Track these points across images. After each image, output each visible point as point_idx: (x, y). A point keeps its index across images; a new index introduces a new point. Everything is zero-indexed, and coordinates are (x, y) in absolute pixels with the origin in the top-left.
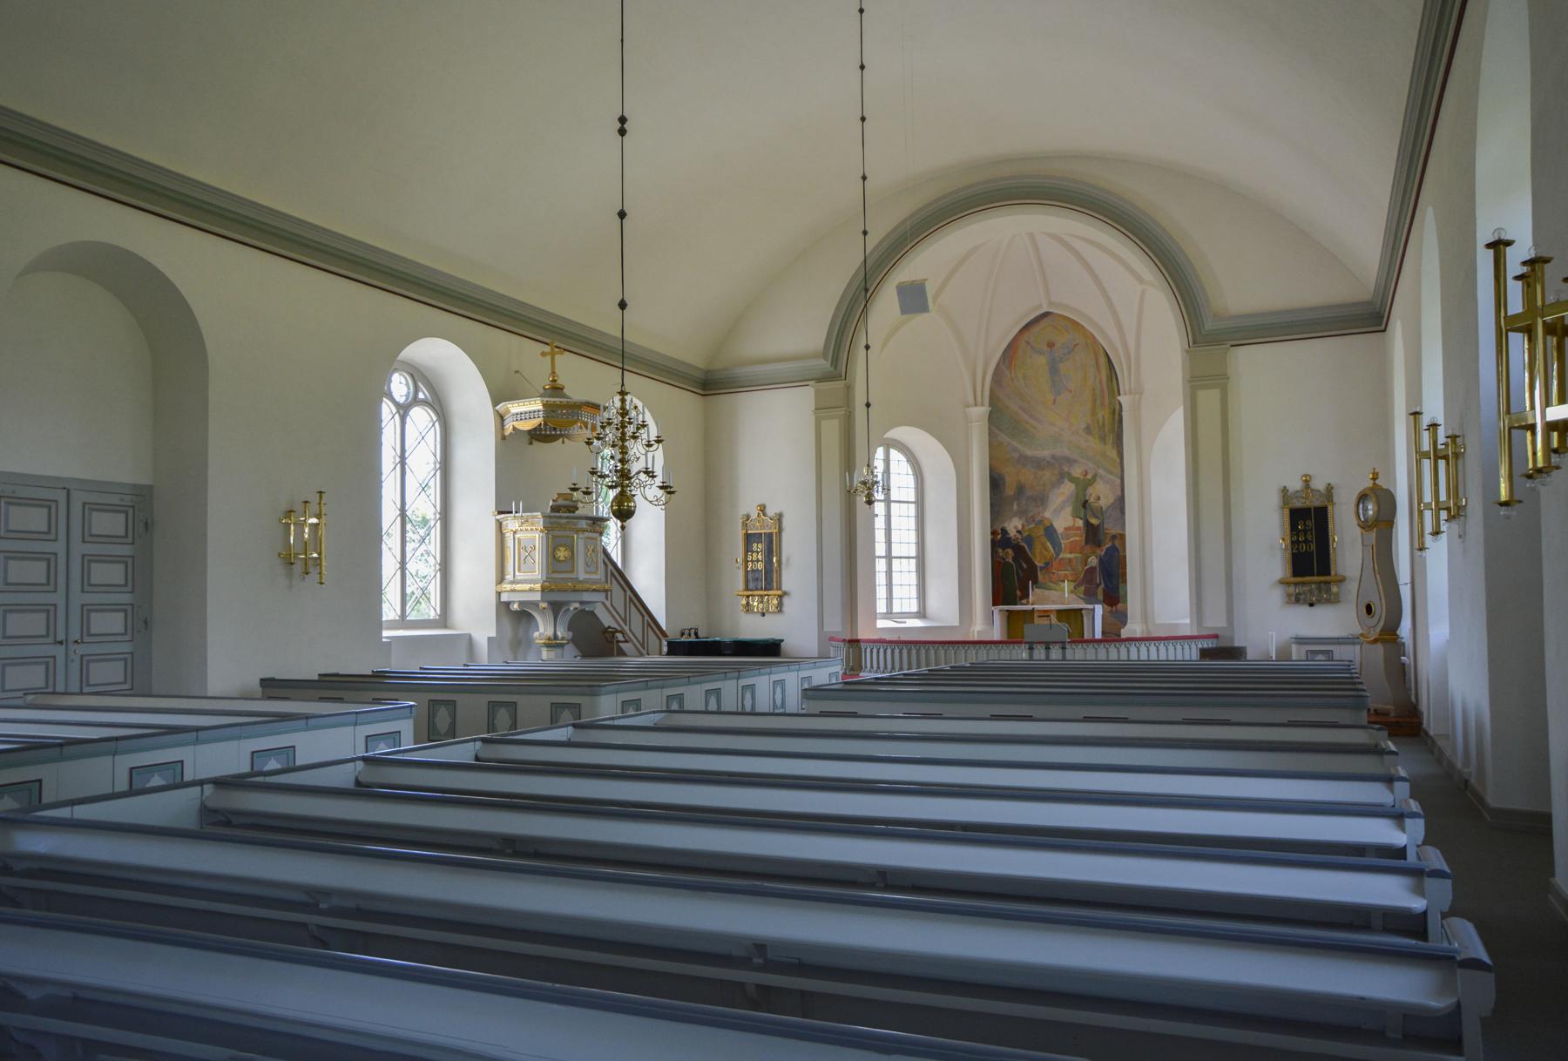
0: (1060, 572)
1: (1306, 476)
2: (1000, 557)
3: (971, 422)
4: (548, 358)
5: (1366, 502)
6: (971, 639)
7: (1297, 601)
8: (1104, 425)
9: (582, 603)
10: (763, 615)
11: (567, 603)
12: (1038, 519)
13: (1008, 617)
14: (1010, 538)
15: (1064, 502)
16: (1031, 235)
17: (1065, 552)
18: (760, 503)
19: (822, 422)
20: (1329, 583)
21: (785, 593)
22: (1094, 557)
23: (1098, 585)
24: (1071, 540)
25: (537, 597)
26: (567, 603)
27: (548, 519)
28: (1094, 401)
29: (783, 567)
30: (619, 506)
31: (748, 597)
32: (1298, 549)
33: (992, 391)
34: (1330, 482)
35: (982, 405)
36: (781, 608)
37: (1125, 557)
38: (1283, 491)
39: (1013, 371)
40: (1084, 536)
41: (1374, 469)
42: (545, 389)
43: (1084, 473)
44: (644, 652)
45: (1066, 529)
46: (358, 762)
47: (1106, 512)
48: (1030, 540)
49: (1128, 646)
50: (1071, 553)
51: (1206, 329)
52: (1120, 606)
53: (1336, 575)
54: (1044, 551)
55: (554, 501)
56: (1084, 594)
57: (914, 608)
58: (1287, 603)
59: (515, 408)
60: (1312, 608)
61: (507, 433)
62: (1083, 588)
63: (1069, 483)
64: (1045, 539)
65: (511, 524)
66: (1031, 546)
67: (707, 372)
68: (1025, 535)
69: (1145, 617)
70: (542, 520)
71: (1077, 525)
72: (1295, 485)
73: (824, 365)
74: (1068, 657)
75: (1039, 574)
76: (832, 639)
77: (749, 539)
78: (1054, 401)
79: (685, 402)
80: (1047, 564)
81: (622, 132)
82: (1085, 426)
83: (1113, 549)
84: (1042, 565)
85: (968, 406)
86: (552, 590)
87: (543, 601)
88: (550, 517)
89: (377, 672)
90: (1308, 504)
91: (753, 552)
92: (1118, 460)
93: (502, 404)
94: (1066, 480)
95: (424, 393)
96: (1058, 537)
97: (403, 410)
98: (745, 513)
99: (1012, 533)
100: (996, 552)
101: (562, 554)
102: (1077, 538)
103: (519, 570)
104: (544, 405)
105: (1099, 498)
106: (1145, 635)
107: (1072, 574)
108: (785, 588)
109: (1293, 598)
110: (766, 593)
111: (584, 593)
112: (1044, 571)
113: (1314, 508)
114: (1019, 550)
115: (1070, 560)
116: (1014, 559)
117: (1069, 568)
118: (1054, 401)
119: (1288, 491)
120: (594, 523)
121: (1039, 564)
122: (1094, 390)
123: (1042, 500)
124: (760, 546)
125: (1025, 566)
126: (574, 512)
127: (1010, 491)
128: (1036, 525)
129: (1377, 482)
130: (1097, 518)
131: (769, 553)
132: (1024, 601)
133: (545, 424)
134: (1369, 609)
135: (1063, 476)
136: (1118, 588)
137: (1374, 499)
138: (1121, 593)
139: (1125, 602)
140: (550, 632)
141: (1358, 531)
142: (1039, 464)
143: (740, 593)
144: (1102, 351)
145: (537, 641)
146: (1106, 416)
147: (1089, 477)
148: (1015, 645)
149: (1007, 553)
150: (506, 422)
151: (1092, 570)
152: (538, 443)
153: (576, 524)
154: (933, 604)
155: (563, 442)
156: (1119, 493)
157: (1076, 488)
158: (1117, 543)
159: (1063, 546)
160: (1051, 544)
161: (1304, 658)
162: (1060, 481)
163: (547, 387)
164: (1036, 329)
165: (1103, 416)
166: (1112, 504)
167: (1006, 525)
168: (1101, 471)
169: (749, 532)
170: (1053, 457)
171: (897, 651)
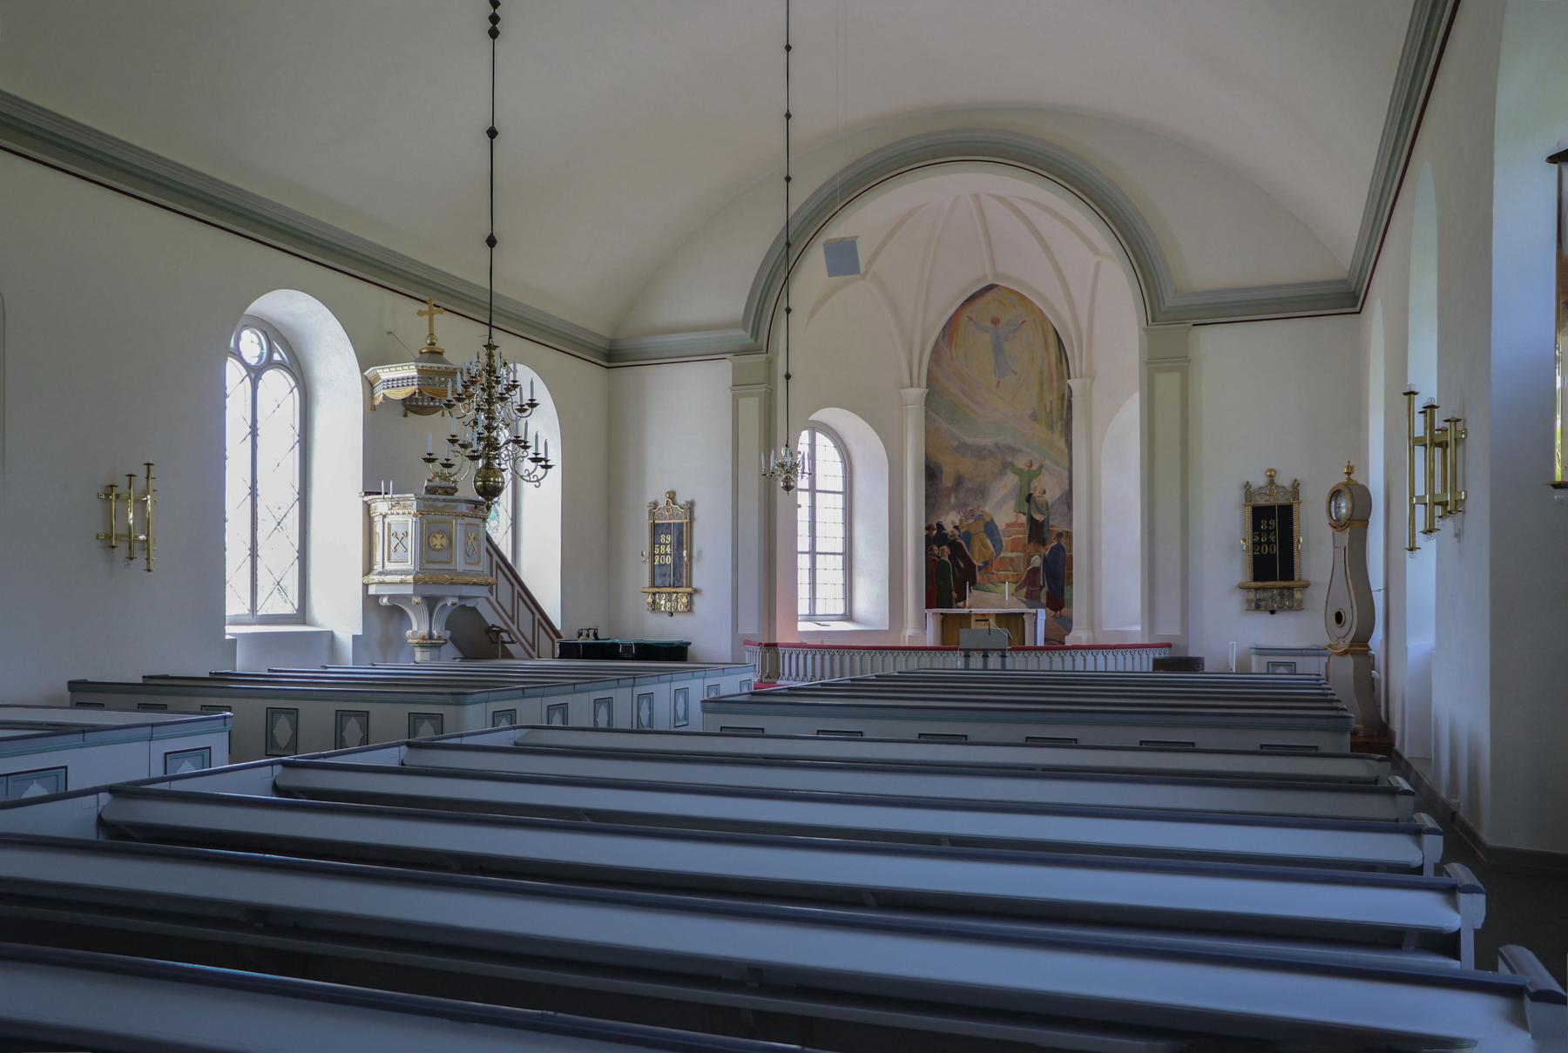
1: (1270, 470)
3: (906, 405)
4: (426, 317)
5: (1339, 498)
6: (902, 645)
7: (1258, 607)
8: (1051, 412)
9: (461, 598)
10: (671, 614)
11: (442, 598)
12: (977, 513)
13: (943, 621)
14: (946, 534)
16: (976, 197)
18: (669, 490)
19: (742, 401)
20: (1292, 588)
21: (696, 591)
23: (1042, 588)
24: (1014, 537)
25: (409, 590)
26: (442, 598)
27: (421, 501)
28: (1042, 384)
29: (694, 561)
30: (484, 482)
31: (654, 594)
32: (1260, 551)
33: (929, 369)
34: (1297, 478)
35: (919, 386)
36: (691, 607)
37: (1071, 557)
38: (1245, 487)
40: (1028, 533)
41: (1349, 462)
42: (421, 353)
43: (1029, 464)
44: (535, 654)
45: (1007, 525)
46: (101, 795)
47: (1052, 505)
48: (968, 536)
50: (1013, 551)
52: (1064, 610)
53: (1300, 580)
54: (983, 548)
55: (429, 481)
56: (1026, 597)
57: (840, 610)
58: (1247, 610)
59: (386, 373)
60: (1274, 616)
61: (377, 402)
62: (1024, 590)
64: (984, 536)
65: (381, 506)
66: (968, 543)
67: (612, 341)
68: (962, 531)
69: (1092, 624)
70: (415, 503)
72: (1259, 481)
73: (744, 336)
74: (1008, 666)
75: (977, 574)
76: (747, 643)
77: (656, 529)
78: (998, 383)
79: (587, 375)
80: (986, 563)
81: (494, 33)
83: (1059, 548)
84: (981, 565)
85: (903, 387)
86: (426, 583)
87: (415, 594)
88: (426, 500)
89: (216, 674)
90: (1272, 501)
91: (660, 544)
92: (1066, 450)
93: (372, 369)
95: (281, 356)
96: (998, 534)
97: (255, 374)
98: (653, 500)
99: (949, 529)
100: (931, 549)
101: (438, 541)
102: (1020, 536)
103: (389, 559)
104: (419, 371)
105: (1044, 492)
106: (1091, 643)
107: (1013, 575)
108: (695, 585)
109: (1253, 605)
110: (674, 590)
111: (464, 587)
112: (983, 571)
113: (1279, 506)
114: (956, 549)
115: (1012, 560)
116: (950, 557)
118: (998, 383)
119: (1250, 487)
120: (476, 507)
121: (977, 563)
122: (1042, 372)
123: (981, 492)
124: (669, 537)
125: (962, 565)
126: (453, 495)
127: (947, 482)
128: (975, 520)
129: (1352, 476)
131: (679, 545)
132: (961, 604)
133: (420, 392)
134: (1339, 618)
135: (1006, 466)
136: (1062, 591)
137: (1348, 496)
138: (1066, 596)
139: (1071, 606)
140: (424, 631)
141: (1330, 530)
142: (980, 453)
143: (646, 590)
144: (1051, 329)
145: (410, 641)
146: (1054, 405)
147: (1034, 468)
148: (950, 652)
149: (943, 550)
150: (376, 390)
151: (1035, 571)
152: (413, 414)
153: (456, 507)
154: (862, 605)
155: (443, 415)
157: (1020, 480)
158: (1063, 542)
160: (992, 541)
161: (1265, 671)
162: (1002, 473)
163: (424, 351)
164: (979, 303)
165: (1051, 402)
166: (1059, 498)
168: (1047, 462)
169: (657, 522)
171: (818, 657)
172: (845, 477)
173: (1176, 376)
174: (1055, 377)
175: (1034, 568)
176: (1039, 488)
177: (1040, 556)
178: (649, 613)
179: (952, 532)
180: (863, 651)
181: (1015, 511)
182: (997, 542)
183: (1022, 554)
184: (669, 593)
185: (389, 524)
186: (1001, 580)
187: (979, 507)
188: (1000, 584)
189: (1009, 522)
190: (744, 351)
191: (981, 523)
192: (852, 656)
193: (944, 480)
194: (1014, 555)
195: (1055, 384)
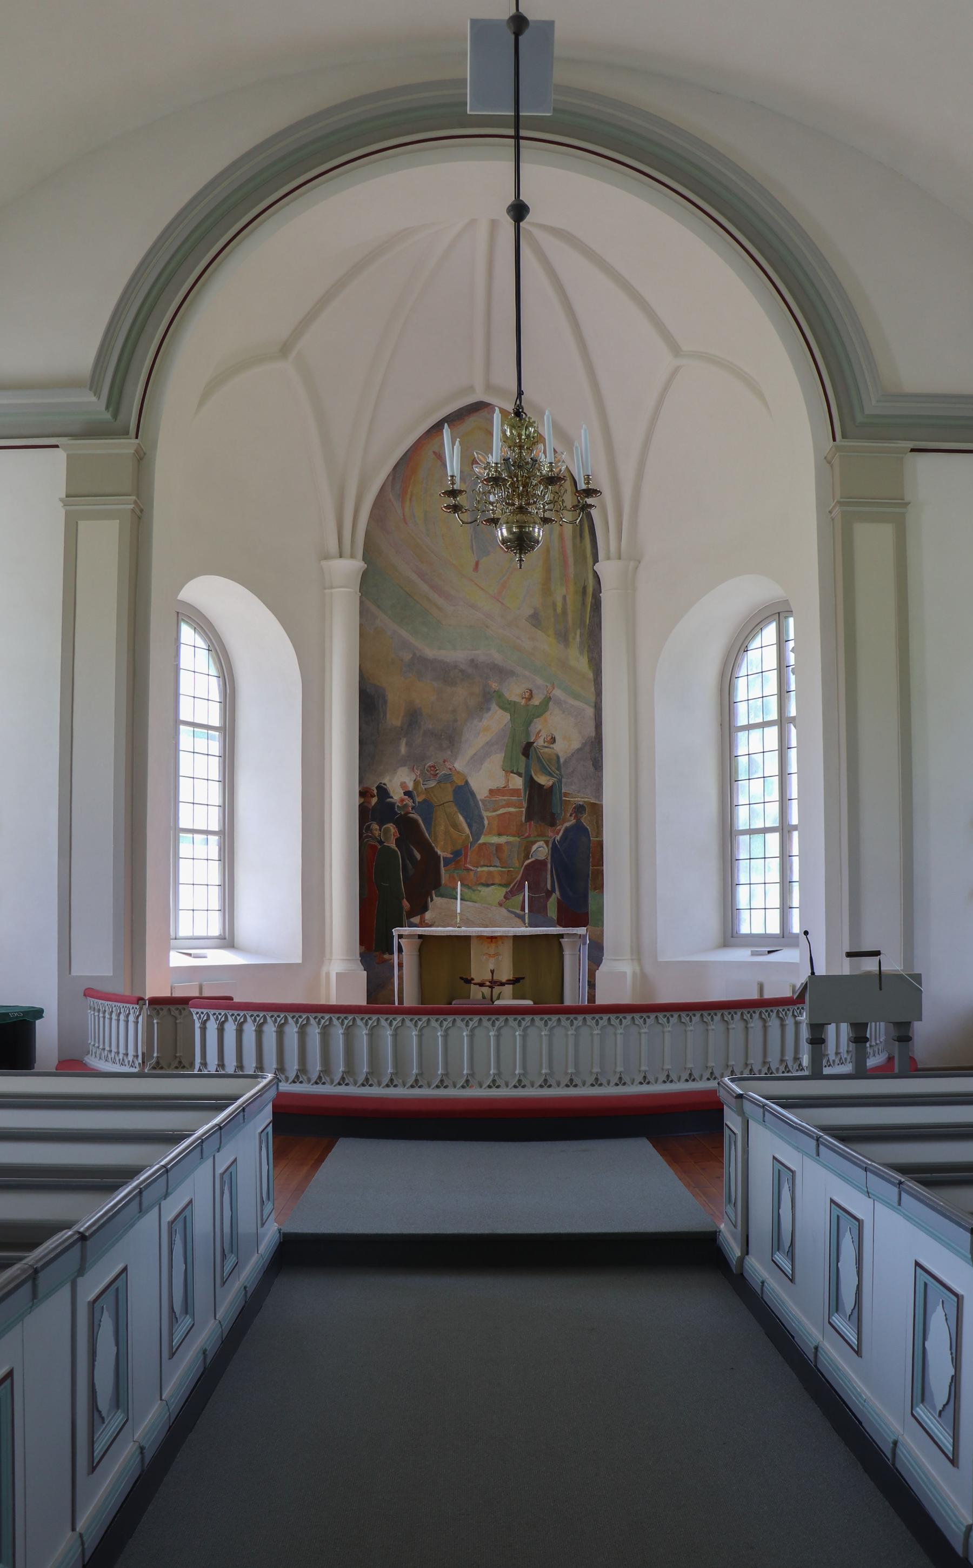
0: (479, 869)
2: (374, 838)
8: (564, 612)
13: (420, 950)
14: (393, 805)
15: (489, 744)
17: (490, 833)
19: (82, 524)
22: (541, 843)
23: (549, 894)
24: (501, 811)
28: (548, 570)
33: (367, 534)
35: (352, 556)
37: (600, 844)
39: (408, 503)
40: (525, 805)
43: (527, 695)
45: (491, 791)
47: (565, 762)
49: (747, 1017)
50: (500, 835)
51: (867, 412)
57: (215, 930)
63: (500, 712)
64: (455, 809)
66: (428, 820)
68: (418, 799)
69: (637, 952)
71: (511, 787)
76: (89, 993)
78: (477, 564)
80: (457, 854)
82: (531, 612)
83: (579, 829)
85: (327, 557)
92: (591, 675)
94: (494, 707)
96: (477, 806)
99: (397, 795)
102: (512, 810)
105: (553, 740)
114: (408, 829)
115: (499, 847)
117: (498, 864)
118: (477, 564)
125: (418, 856)
127: (394, 718)
128: (439, 782)
130: (550, 775)
132: (416, 920)
135: (488, 698)
136: (586, 897)
138: (592, 906)
139: (600, 922)
146: (569, 601)
147: (536, 701)
149: (387, 830)
151: (538, 866)
156: (591, 731)
158: (585, 820)
159: (486, 822)
160: (465, 818)
165: (564, 598)
166: (579, 750)
167: (386, 780)
168: (558, 693)
170: (473, 663)
172: (223, 703)
173: (886, 531)
174: (571, 560)
175: (537, 859)
176: (543, 734)
177: (547, 843)
179: (402, 800)
180: (327, 1016)
181: (506, 772)
182: (474, 818)
183: (517, 839)
186: (483, 881)
187: (444, 762)
188: (479, 888)
189: (494, 787)
190: (92, 431)
191: (450, 789)
192: (348, 1028)
193: (388, 716)
194: (502, 840)
195: (571, 570)
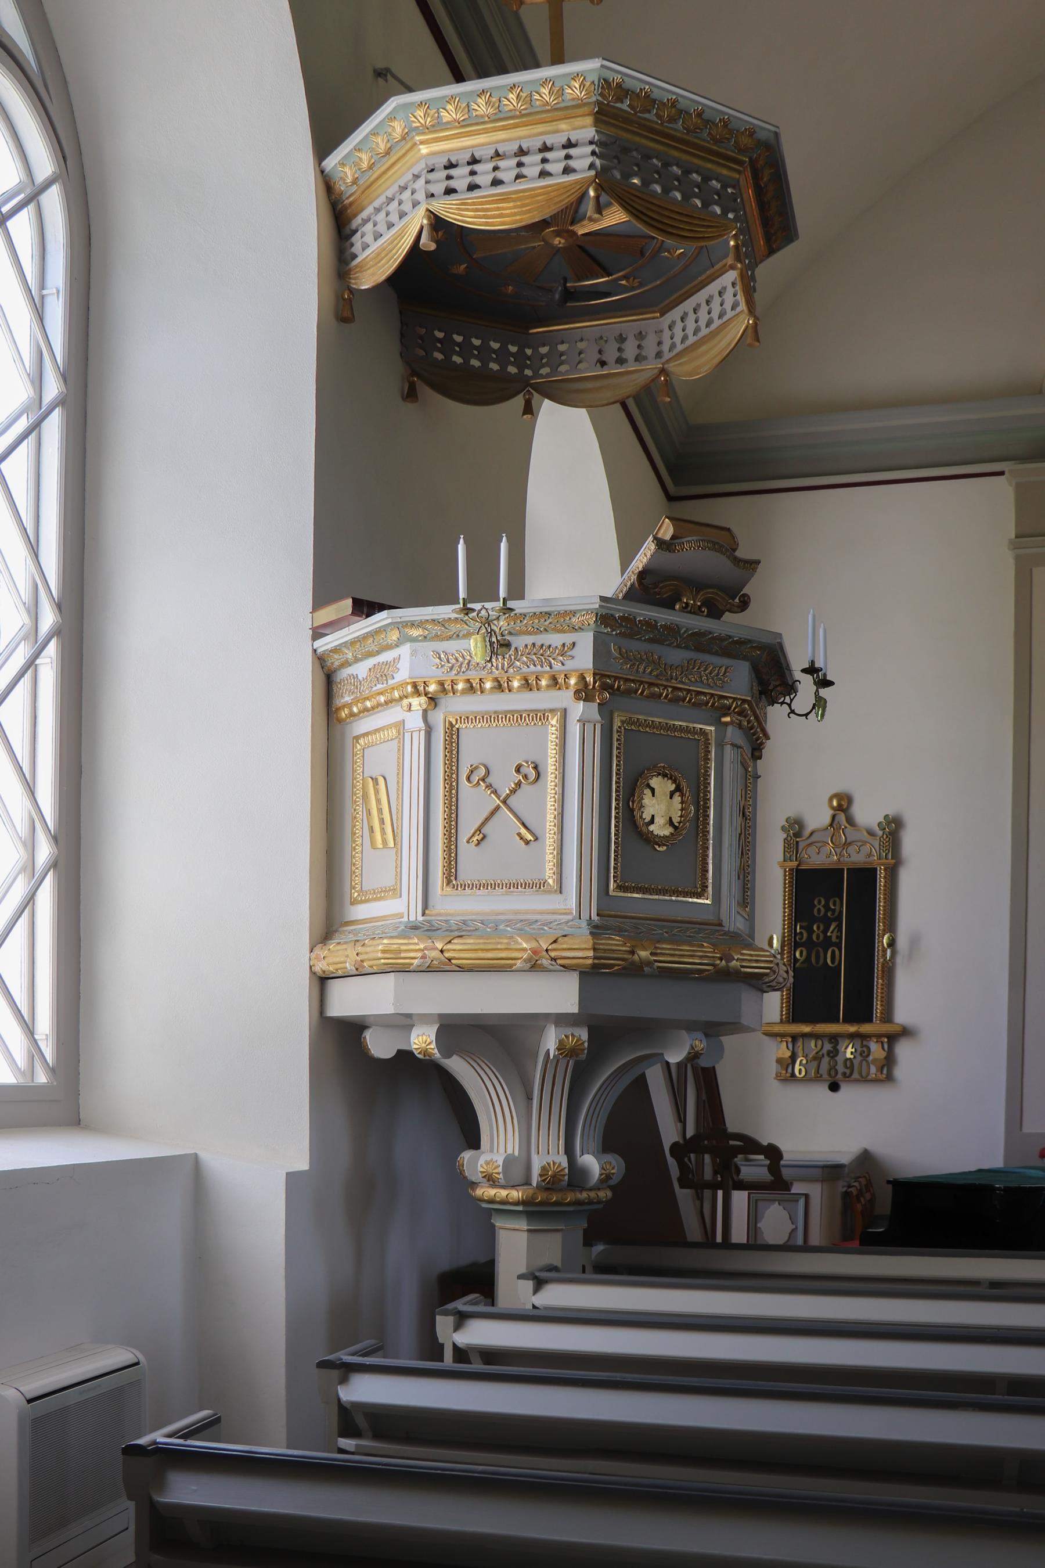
10: (834, 1087)
21: (906, 1032)
29: (899, 960)
31: (795, 1038)
55: (660, 543)
98: (792, 813)
103: (451, 875)
108: (902, 1015)
110: (852, 1029)
143: (777, 1029)
178: (776, 1083)
184: (834, 1038)
185: (453, 735)
